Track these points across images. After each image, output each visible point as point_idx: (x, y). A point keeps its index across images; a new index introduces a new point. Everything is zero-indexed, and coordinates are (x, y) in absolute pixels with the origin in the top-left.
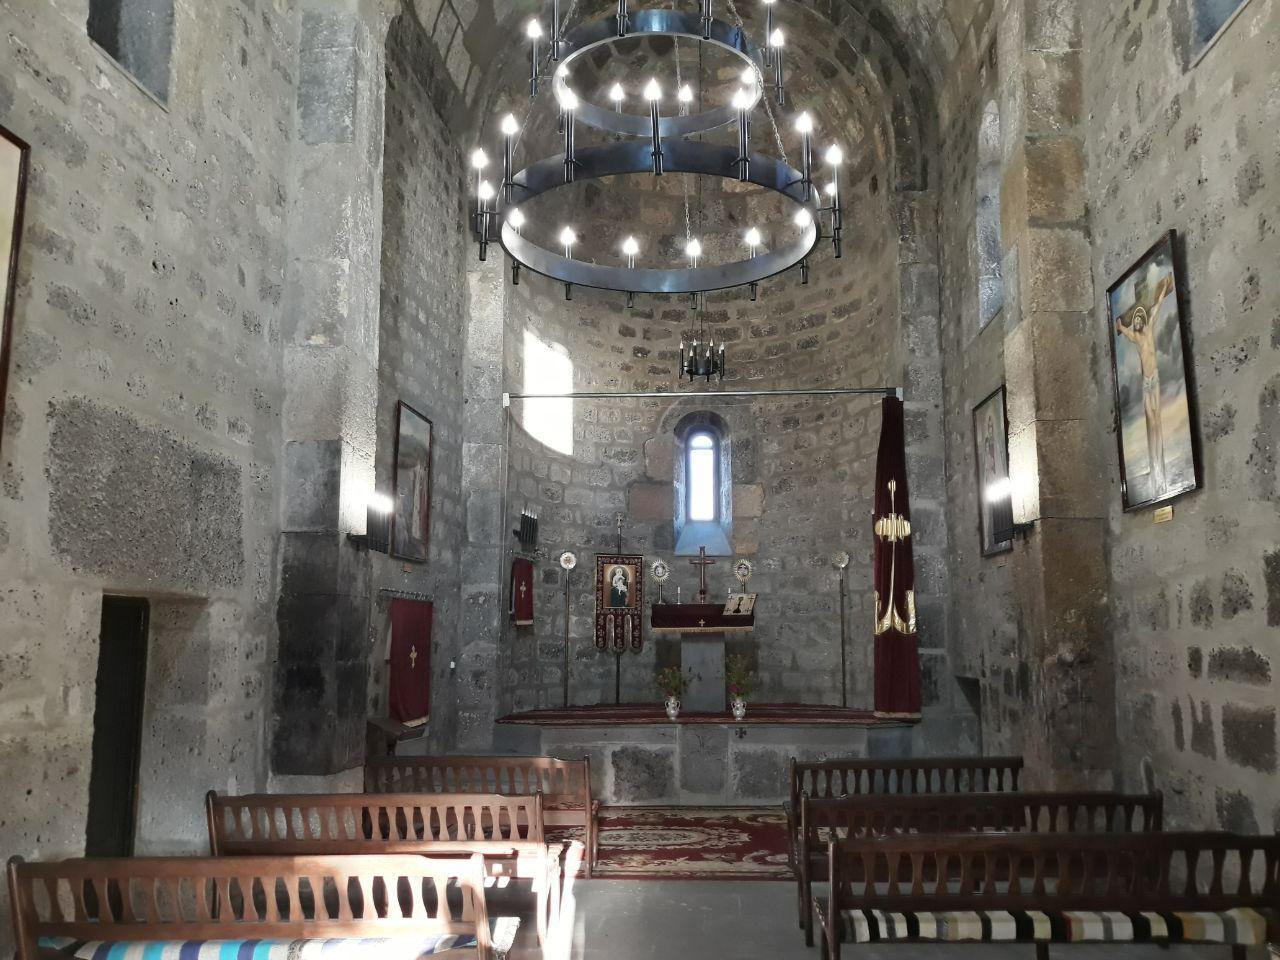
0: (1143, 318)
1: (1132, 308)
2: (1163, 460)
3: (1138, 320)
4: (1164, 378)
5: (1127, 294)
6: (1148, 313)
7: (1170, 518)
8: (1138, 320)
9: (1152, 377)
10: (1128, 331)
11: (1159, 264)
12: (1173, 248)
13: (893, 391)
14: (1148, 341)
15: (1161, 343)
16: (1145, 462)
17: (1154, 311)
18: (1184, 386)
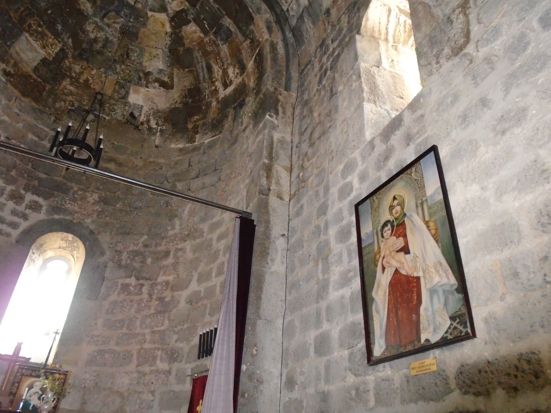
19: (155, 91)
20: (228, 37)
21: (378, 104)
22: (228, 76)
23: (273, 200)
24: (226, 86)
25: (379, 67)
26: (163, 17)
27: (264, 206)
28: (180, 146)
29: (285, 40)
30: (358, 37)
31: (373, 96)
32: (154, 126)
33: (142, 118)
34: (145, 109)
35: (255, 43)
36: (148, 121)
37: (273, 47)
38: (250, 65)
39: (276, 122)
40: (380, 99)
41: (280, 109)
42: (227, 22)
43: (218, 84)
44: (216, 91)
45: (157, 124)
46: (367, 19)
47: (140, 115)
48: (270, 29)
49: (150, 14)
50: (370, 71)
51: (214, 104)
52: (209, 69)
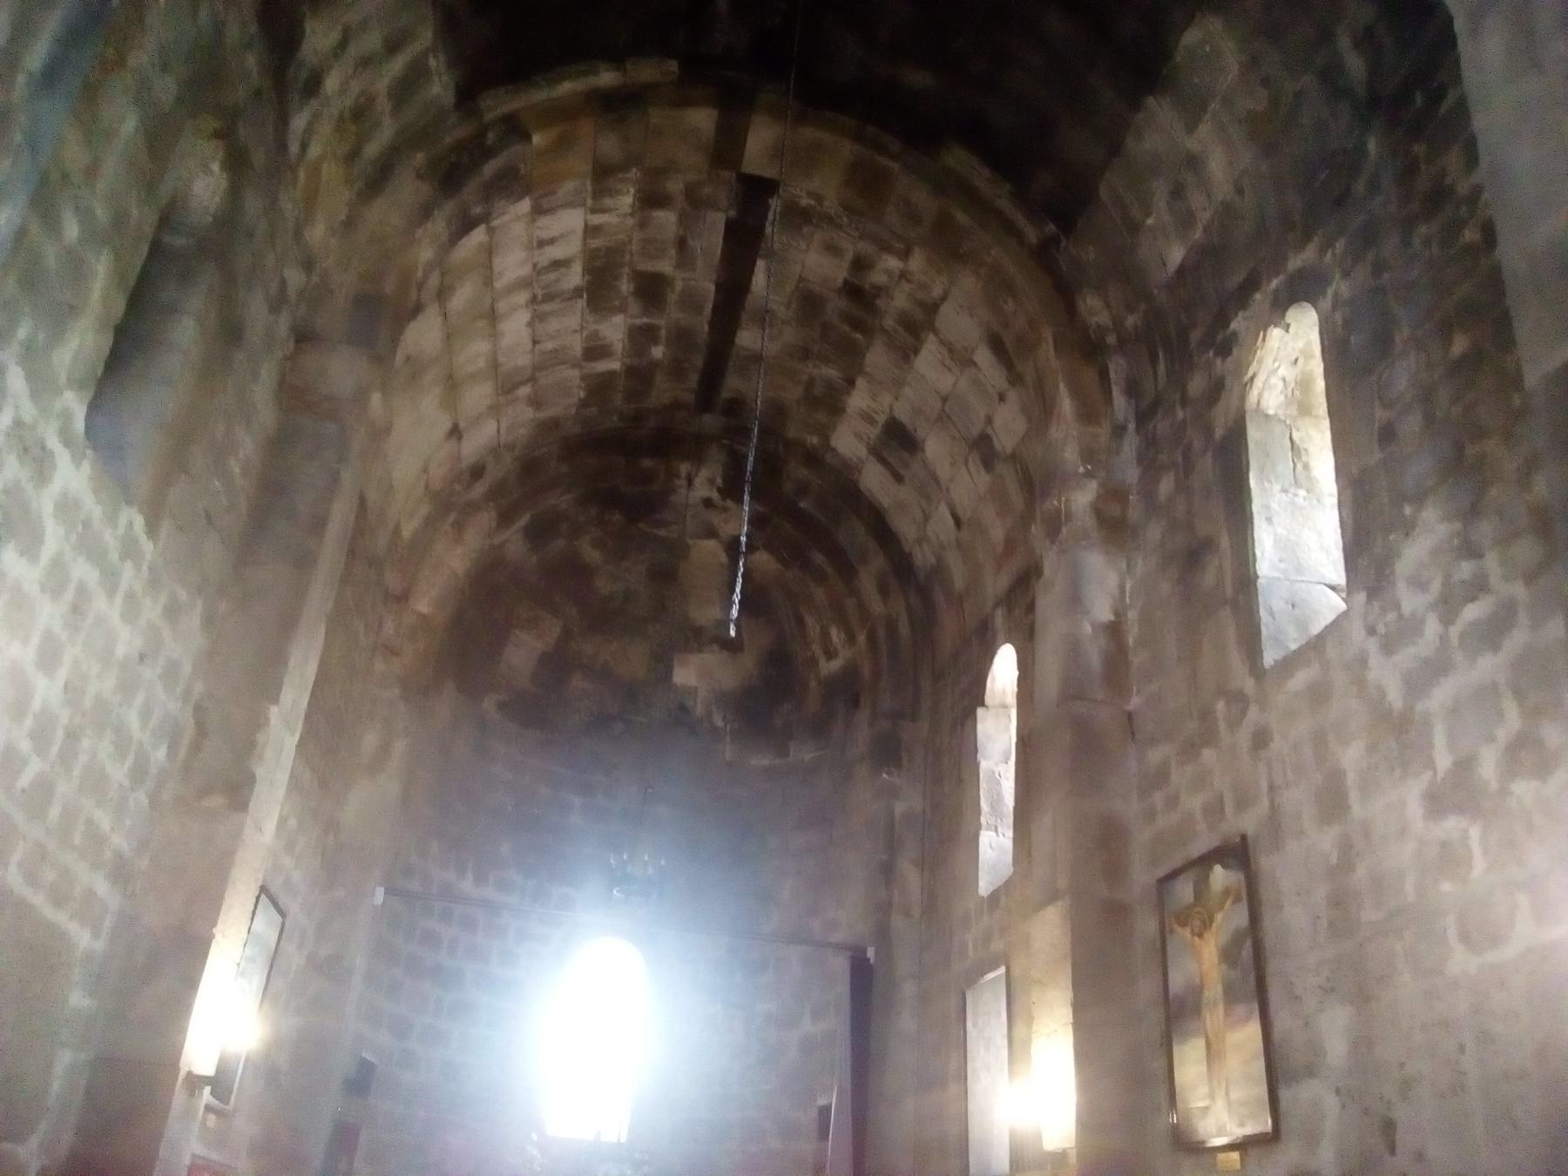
0: (1203, 922)
1: (1189, 907)
2: (1227, 1094)
3: (1197, 923)
4: (1231, 995)
5: (1184, 891)
6: (1211, 920)
7: (1238, 1166)
8: (1197, 923)
9: (1214, 991)
10: (1185, 933)
11: (1225, 866)
12: (1237, 853)
13: (864, 951)
14: (1209, 952)
15: (1229, 955)
16: (1203, 1090)
17: (1219, 917)
18: (1257, 1013)
19: (711, 658)
20: (821, 578)
21: (1000, 829)
22: (831, 639)
23: (897, 921)
24: (830, 654)
25: (1007, 763)
26: (711, 544)
27: (883, 934)
28: (766, 762)
29: (909, 610)
30: (980, 712)
31: (994, 818)
32: (719, 723)
33: (699, 710)
34: (702, 693)
35: (862, 607)
36: (709, 715)
37: (892, 627)
38: (862, 638)
39: (897, 781)
40: (1004, 820)
41: (904, 755)
42: (818, 558)
43: (817, 649)
44: (813, 662)
45: (724, 718)
46: (994, 679)
47: (696, 706)
48: (884, 591)
49: (690, 542)
50: (993, 773)
51: (813, 684)
52: (800, 621)
